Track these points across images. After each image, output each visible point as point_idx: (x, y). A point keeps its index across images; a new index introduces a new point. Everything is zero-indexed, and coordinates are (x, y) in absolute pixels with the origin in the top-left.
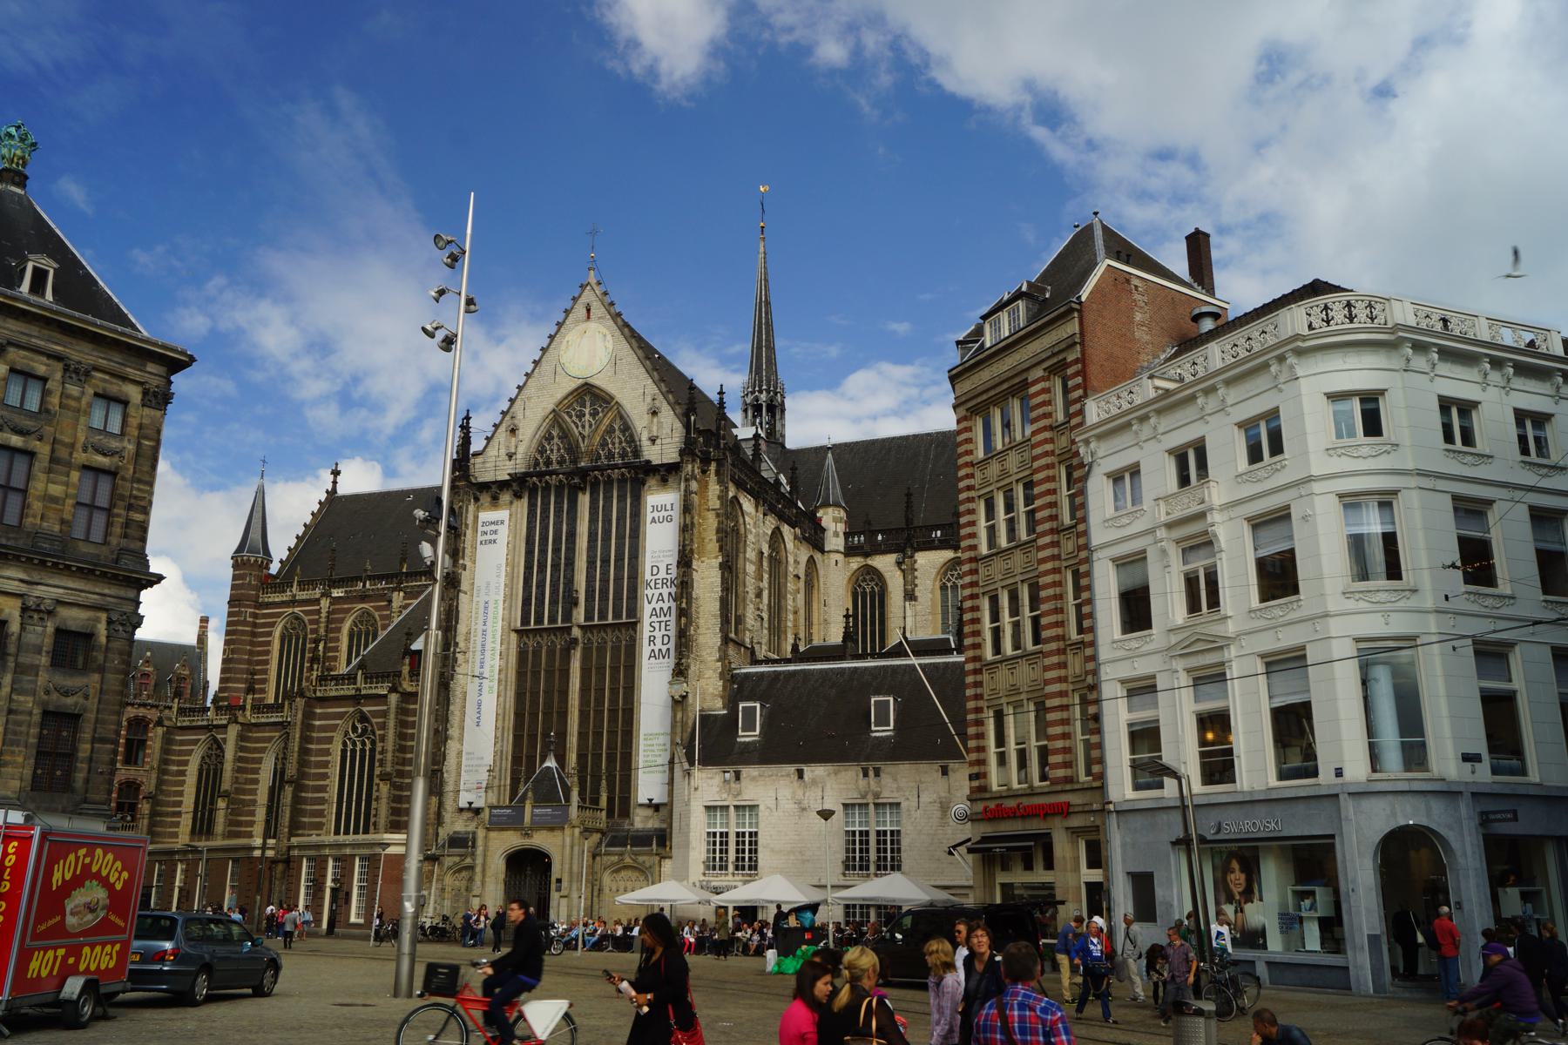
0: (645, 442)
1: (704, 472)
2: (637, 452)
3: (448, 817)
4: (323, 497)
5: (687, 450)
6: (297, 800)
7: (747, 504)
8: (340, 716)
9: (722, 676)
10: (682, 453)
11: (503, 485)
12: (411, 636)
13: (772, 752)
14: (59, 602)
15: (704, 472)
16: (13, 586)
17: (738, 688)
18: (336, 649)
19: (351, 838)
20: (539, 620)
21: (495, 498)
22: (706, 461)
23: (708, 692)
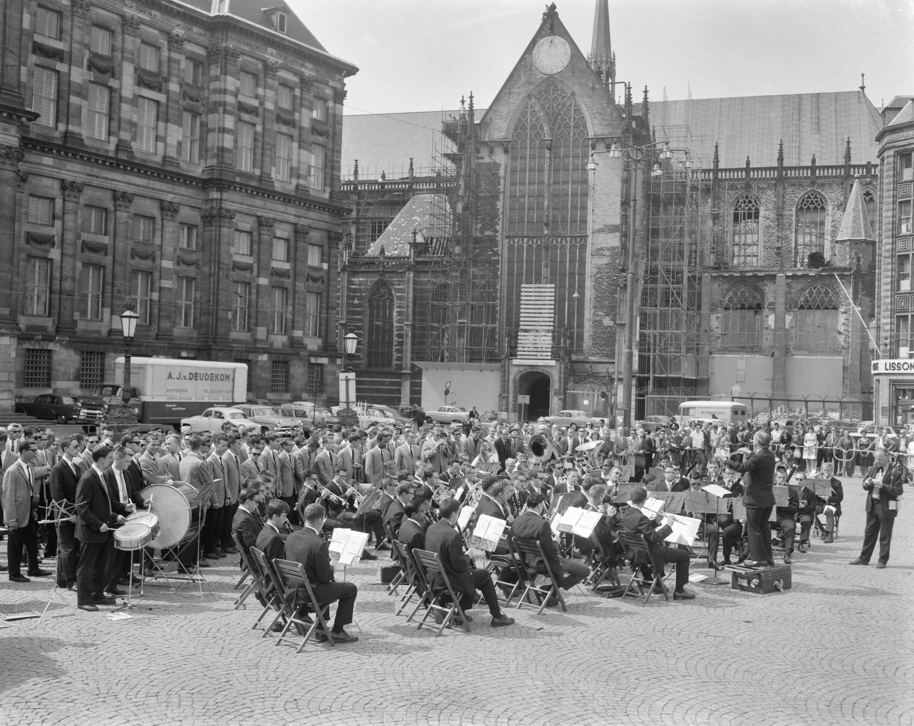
12: (415, 233)
14: (310, 227)
16: (292, 219)
21: (491, 152)
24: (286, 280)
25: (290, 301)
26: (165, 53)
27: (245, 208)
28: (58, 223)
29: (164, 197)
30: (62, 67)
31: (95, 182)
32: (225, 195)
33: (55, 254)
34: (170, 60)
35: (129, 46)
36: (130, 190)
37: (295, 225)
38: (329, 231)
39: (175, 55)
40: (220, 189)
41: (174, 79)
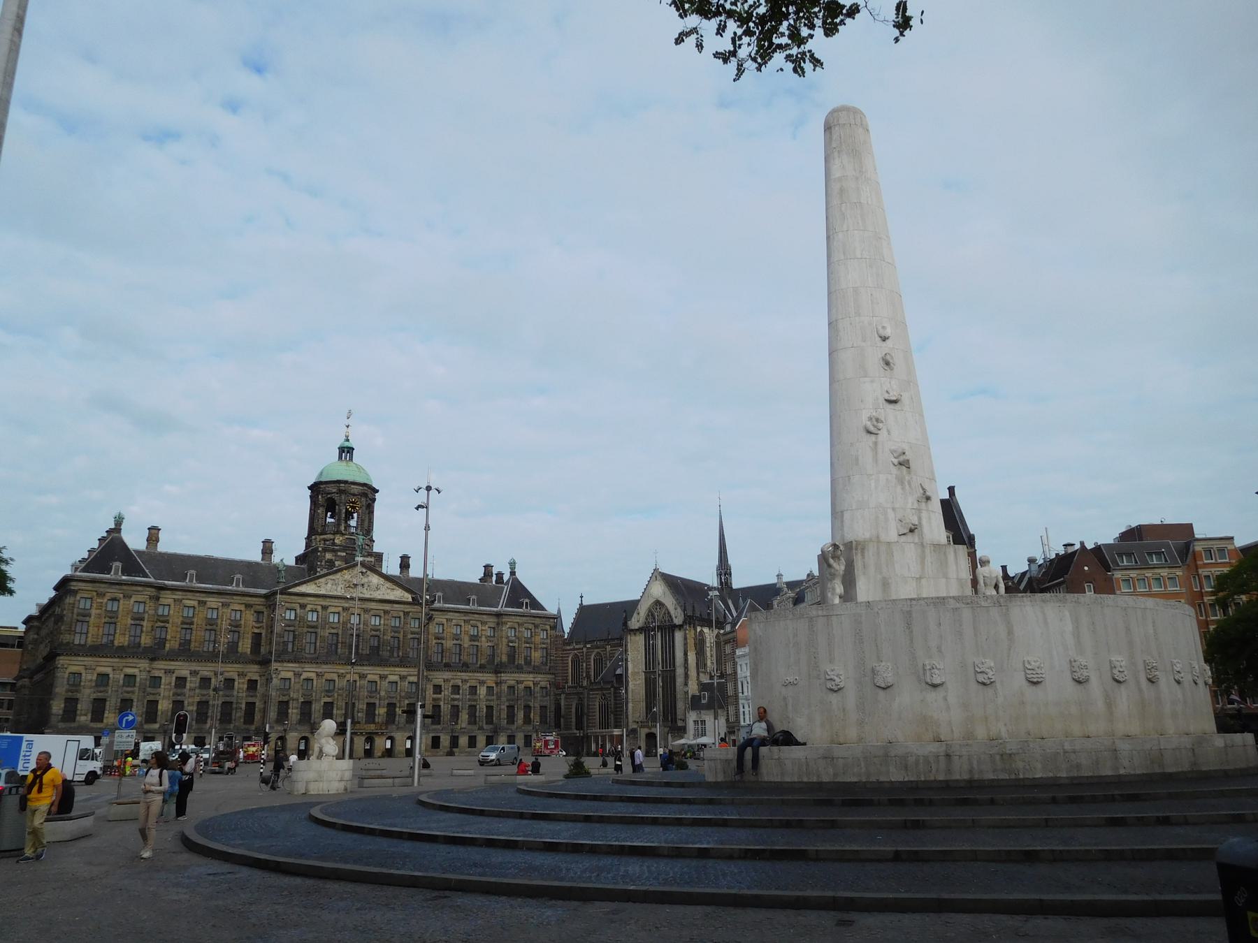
0: (674, 619)
1: (690, 627)
2: (672, 620)
3: (630, 724)
4: (578, 607)
5: (685, 622)
6: (588, 719)
7: (706, 630)
8: (597, 694)
9: (698, 685)
10: (683, 622)
11: (637, 630)
12: (615, 670)
13: (709, 707)
15: (690, 627)
17: (703, 687)
18: (590, 665)
19: (604, 730)
20: (650, 669)
21: (635, 634)
22: (690, 624)
23: (693, 688)
24: (529, 703)
25: (532, 711)
26: (480, 629)
27: (512, 678)
28: (443, 693)
29: (479, 678)
30: (444, 642)
31: (455, 677)
32: (502, 675)
33: (442, 703)
34: (482, 630)
35: (467, 629)
36: (467, 678)
37: (533, 681)
38: (549, 681)
39: (483, 628)
40: (501, 673)
41: (483, 636)
